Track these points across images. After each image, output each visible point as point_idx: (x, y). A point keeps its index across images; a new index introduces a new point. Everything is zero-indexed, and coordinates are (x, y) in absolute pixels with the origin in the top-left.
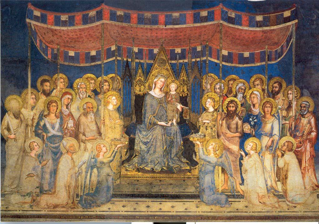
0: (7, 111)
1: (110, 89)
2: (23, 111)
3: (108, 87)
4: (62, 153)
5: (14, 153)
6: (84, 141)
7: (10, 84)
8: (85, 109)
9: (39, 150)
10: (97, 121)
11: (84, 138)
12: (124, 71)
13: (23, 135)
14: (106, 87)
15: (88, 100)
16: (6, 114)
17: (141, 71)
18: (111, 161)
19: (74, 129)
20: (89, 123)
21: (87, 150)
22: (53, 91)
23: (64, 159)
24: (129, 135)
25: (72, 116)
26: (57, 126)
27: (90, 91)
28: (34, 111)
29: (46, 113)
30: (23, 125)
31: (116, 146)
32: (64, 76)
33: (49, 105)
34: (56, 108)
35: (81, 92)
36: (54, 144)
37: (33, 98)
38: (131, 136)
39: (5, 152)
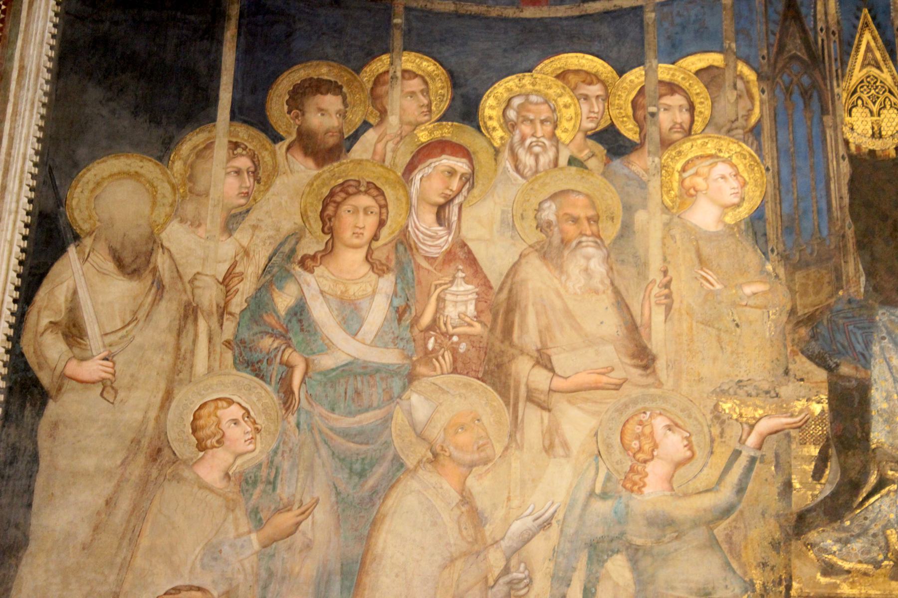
0: (77, 238)
1: (698, 126)
2: (176, 236)
3: (685, 117)
4: (398, 464)
5: (89, 463)
6: (542, 397)
7: (113, 104)
8: (549, 224)
9: (251, 447)
10: (622, 289)
11: (540, 379)
12: (772, 38)
13: (163, 360)
14: (670, 114)
15: (569, 179)
16: (72, 250)
17: (874, 38)
18: (727, 511)
19: (478, 328)
20: (571, 302)
21: (560, 451)
22: (362, 138)
23: (411, 501)
24: (829, 369)
25: (472, 261)
26: (377, 313)
27: (580, 136)
28: (237, 235)
29: (311, 246)
30: (167, 313)
31: (752, 427)
32: (428, 66)
33: (330, 210)
34: (371, 222)
35: (523, 139)
36: (350, 414)
37: (238, 172)
38: (845, 370)
39: (35, 458)
